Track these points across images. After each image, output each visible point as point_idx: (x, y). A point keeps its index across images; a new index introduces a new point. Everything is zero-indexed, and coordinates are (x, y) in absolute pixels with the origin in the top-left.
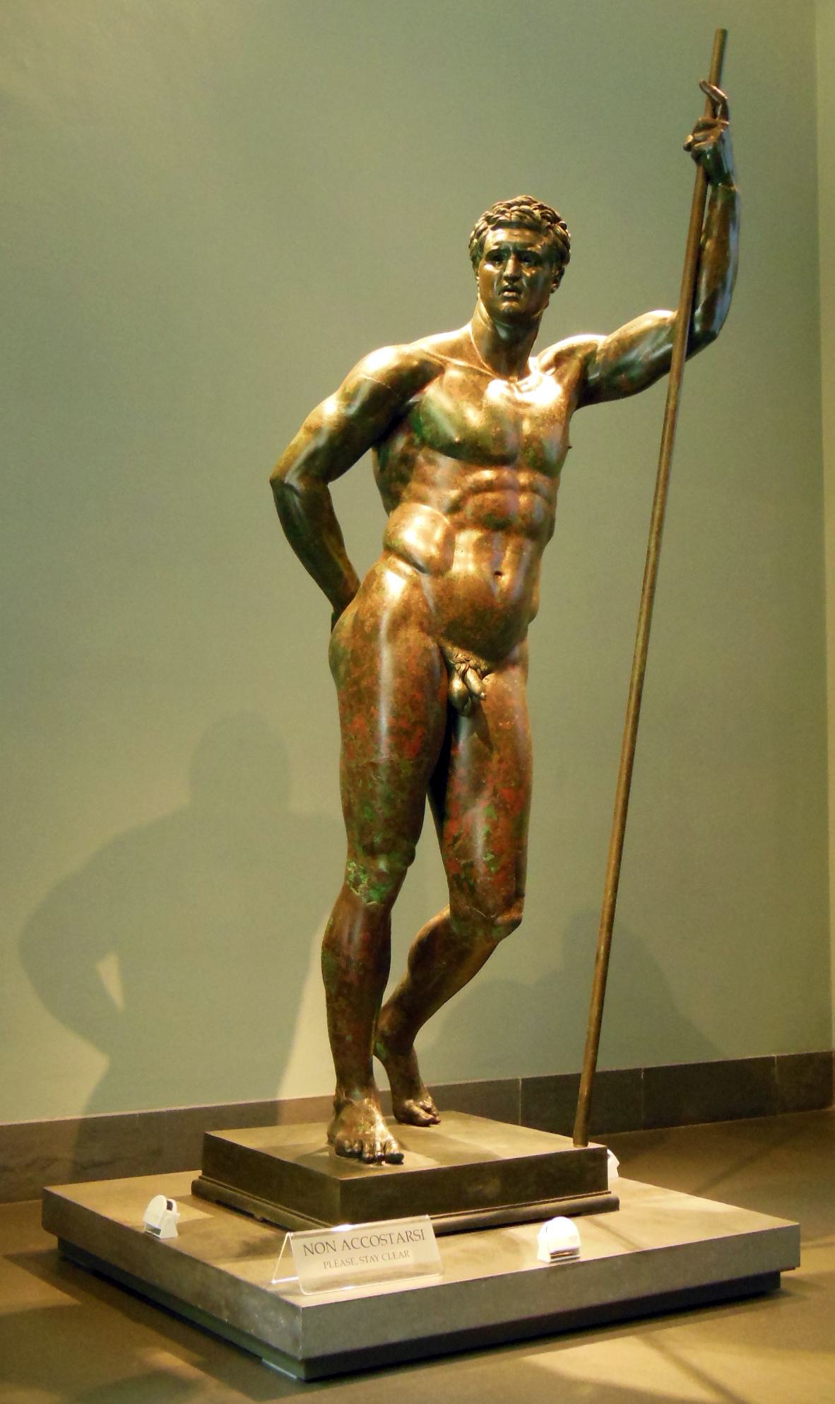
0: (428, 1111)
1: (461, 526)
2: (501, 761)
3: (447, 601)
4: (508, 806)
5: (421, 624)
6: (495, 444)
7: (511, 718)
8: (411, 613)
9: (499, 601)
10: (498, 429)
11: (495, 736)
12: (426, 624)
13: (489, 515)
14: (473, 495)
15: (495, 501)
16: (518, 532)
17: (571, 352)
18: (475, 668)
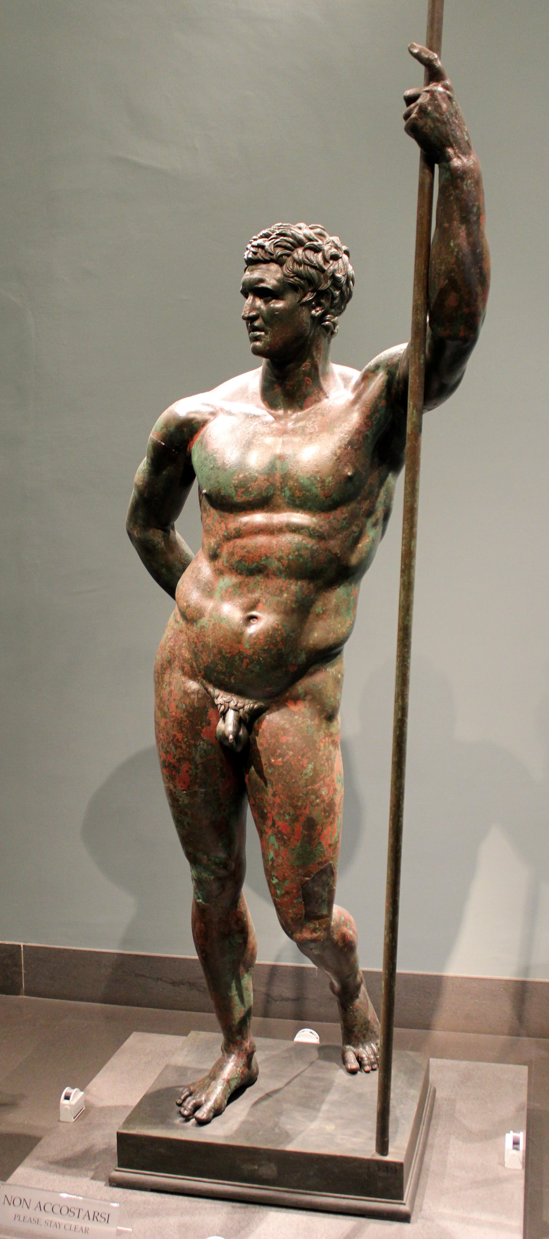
0: (359, 1059)
1: (219, 573)
2: (274, 795)
3: (200, 648)
4: (285, 837)
5: (183, 669)
6: (236, 491)
8: (175, 658)
10: (241, 476)
11: (268, 771)
12: (187, 667)
13: (240, 561)
14: (227, 542)
15: (243, 547)
16: (277, 574)
17: (377, 367)
18: (236, 710)
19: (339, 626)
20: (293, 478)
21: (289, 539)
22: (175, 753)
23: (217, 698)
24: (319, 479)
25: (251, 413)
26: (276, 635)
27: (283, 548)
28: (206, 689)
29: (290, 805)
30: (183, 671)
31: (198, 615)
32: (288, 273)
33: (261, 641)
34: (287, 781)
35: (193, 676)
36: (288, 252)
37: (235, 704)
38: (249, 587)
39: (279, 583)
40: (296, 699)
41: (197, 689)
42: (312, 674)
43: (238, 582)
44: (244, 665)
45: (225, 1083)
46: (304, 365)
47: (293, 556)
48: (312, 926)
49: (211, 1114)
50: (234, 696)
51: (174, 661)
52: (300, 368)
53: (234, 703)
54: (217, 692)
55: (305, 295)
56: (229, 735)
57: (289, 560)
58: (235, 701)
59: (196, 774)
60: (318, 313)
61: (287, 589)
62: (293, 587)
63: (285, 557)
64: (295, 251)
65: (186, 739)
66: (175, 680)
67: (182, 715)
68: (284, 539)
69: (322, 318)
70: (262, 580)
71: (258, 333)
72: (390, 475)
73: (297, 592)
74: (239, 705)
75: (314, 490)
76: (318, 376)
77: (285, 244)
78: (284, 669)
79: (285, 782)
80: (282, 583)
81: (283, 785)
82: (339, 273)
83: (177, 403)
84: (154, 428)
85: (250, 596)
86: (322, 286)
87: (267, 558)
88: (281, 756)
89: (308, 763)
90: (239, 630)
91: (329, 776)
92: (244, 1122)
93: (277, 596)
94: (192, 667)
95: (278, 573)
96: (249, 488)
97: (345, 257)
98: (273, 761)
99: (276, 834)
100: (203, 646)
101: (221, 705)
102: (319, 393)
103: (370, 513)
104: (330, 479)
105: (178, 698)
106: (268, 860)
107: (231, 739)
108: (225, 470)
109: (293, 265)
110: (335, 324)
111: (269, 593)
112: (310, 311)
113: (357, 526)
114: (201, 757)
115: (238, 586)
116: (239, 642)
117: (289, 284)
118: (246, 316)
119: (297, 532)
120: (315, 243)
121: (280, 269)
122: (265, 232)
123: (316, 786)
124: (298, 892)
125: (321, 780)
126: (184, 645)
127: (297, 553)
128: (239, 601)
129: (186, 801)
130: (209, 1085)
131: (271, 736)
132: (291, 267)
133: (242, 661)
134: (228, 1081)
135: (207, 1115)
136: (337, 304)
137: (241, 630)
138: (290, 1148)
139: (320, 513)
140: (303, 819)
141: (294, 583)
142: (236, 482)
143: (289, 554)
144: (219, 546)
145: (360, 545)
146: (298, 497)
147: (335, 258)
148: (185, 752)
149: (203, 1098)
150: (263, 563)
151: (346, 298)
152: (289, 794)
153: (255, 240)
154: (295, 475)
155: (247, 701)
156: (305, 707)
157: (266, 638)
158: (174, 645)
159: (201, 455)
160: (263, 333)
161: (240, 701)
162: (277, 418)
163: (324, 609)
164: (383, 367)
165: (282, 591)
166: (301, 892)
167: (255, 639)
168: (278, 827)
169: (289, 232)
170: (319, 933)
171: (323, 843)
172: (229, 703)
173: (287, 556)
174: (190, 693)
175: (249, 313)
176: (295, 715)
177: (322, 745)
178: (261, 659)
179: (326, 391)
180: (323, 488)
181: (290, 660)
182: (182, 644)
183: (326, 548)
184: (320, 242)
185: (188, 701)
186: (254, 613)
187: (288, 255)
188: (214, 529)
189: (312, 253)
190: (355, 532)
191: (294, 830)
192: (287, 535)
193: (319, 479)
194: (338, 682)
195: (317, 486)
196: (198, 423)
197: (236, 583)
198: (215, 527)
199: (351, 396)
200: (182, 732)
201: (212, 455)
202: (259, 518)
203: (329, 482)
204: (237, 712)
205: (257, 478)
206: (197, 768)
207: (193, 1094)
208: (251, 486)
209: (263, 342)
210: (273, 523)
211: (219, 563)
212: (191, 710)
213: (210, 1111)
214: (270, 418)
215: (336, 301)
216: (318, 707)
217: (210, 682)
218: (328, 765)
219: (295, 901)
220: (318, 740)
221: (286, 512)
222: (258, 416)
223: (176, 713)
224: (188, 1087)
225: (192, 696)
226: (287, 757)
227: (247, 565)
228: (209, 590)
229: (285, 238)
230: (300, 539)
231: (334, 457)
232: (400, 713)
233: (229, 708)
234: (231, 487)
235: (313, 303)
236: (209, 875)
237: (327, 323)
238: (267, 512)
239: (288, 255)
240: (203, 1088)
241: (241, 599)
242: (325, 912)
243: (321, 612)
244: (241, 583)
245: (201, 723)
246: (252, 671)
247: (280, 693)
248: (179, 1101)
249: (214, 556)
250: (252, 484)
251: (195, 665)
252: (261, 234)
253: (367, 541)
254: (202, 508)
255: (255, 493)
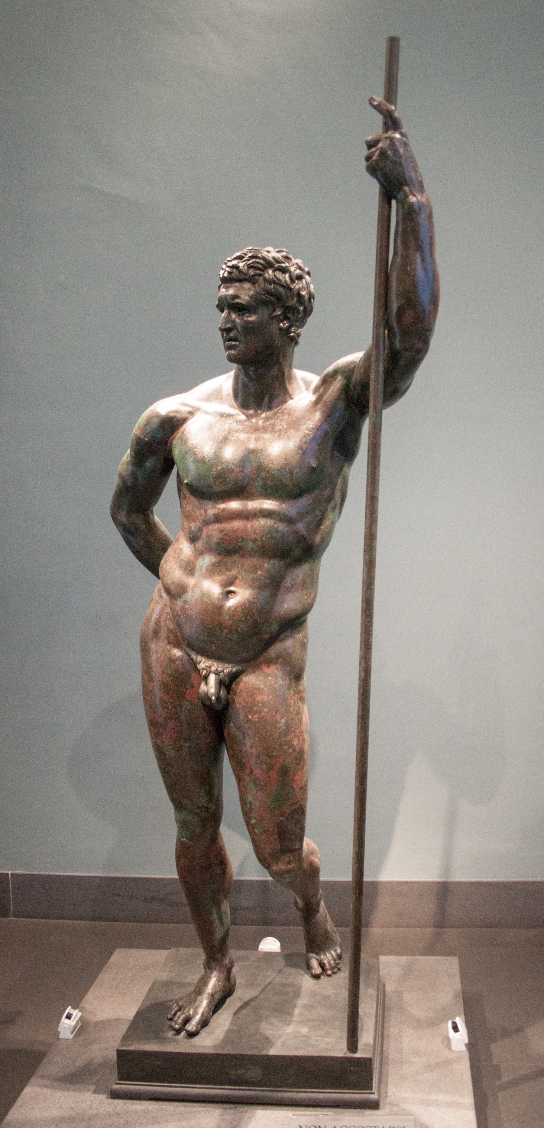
1: (199, 553)
4: (262, 783)
5: (168, 638)
7: (258, 712)
8: (160, 629)
9: (227, 618)
10: (219, 468)
16: (252, 553)
17: (335, 373)
18: (217, 673)
19: (306, 598)
20: (265, 470)
21: (262, 523)
22: (162, 713)
23: (199, 664)
24: (288, 470)
25: (226, 412)
26: (252, 608)
27: (257, 531)
28: (189, 656)
29: (266, 756)
30: (168, 641)
31: (182, 591)
32: (260, 290)
33: (239, 613)
34: (264, 734)
35: (177, 645)
36: (259, 272)
37: (216, 668)
38: (227, 566)
39: (254, 562)
40: (269, 662)
41: (181, 656)
42: (283, 640)
43: (217, 561)
44: (224, 633)
45: (210, 997)
46: (272, 370)
47: (266, 538)
48: (287, 859)
49: (200, 1026)
50: (215, 661)
51: (160, 632)
52: (269, 374)
53: (215, 667)
54: (199, 658)
55: (274, 310)
56: (212, 697)
57: (262, 541)
58: (215, 666)
59: (182, 730)
60: (285, 326)
61: (261, 567)
62: (266, 565)
63: (259, 539)
64: (266, 272)
65: (172, 701)
66: (160, 649)
67: (168, 679)
68: (257, 524)
69: (288, 330)
70: (238, 559)
71: (233, 343)
72: (346, 465)
73: (269, 570)
74: (220, 669)
75: (284, 480)
76: (284, 379)
77: (257, 265)
78: (259, 637)
79: (262, 735)
80: (256, 562)
81: (259, 738)
82: (303, 291)
83: (157, 402)
84: (137, 426)
85: (228, 573)
86: (289, 302)
87: (243, 540)
88: (256, 712)
89: (281, 718)
90: (219, 604)
91: (299, 728)
92: (229, 1031)
93: (252, 573)
94: (176, 636)
95: (253, 553)
96: (226, 478)
97: (307, 277)
98: (250, 717)
99: (254, 781)
100: (186, 618)
101: (203, 669)
102: (285, 395)
103: (330, 499)
104: (298, 470)
105: (164, 664)
106: (247, 803)
107: (214, 700)
108: (205, 463)
109: (265, 285)
110: (298, 335)
111: (245, 570)
112: (279, 323)
113: (320, 510)
114: (185, 716)
115: (217, 565)
116: (220, 614)
117: (261, 300)
118: (223, 327)
119: (269, 517)
120: (283, 265)
121: (252, 287)
122: (238, 254)
123: (289, 738)
124: (274, 830)
125: (292, 733)
126: (168, 617)
127: (269, 535)
128: (218, 578)
129: (173, 755)
130: (196, 1000)
131: (249, 696)
132: (263, 286)
133: (222, 631)
134: (212, 995)
135: (196, 1028)
136: (301, 318)
137: (221, 603)
138: (272, 1052)
139: (288, 500)
140: (278, 766)
141: (267, 562)
142: (215, 473)
143: (262, 536)
144: (200, 530)
145: (322, 527)
146: (270, 487)
147: (300, 278)
148: (171, 712)
149: (191, 1012)
150: (239, 544)
151: (308, 312)
152: (265, 745)
153: (229, 261)
154: (267, 467)
155: (226, 665)
156: (277, 669)
157: (243, 610)
158: (160, 618)
159: (182, 449)
160: (237, 343)
161: (220, 666)
162: (249, 417)
163: (292, 583)
164: (341, 373)
165: (256, 569)
166: (276, 830)
167: (233, 611)
168: (255, 775)
169: (260, 255)
170: (293, 865)
171: (295, 786)
172: (210, 667)
173: (261, 539)
174: (175, 660)
175: (225, 325)
176: (268, 676)
177: (292, 701)
178: (239, 629)
179: (291, 393)
180: (291, 478)
181: (264, 628)
182: (167, 616)
183: (294, 531)
184: (287, 264)
185: (173, 667)
186: (232, 588)
187: (260, 275)
188: (194, 515)
189: (281, 273)
190: (318, 516)
191: (270, 777)
192: (260, 520)
193: (288, 470)
194: (304, 646)
195: (286, 477)
196: (178, 421)
197: (215, 562)
198: (195, 513)
199: (313, 398)
200: (168, 694)
201: (192, 450)
202: (234, 505)
203: (297, 473)
204: (218, 676)
205: (233, 470)
206: (182, 726)
207: (182, 1009)
208: (228, 477)
209: (237, 351)
210: (248, 510)
211: (200, 544)
212: (176, 675)
213: (198, 1024)
214: (243, 417)
215: (300, 316)
216: (288, 668)
217: (193, 649)
218: (298, 719)
219: (271, 838)
220: (289, 698)
221: (259, 499)
222: (232, 415)
223: (162, 678)
224: (177, 1001)
225: (177, 662)
226: (263, 714)
227: (225, 546)
228: (190, 568)
229: (257, 260)
230: (272, 523)
231: (300, 451)
232: (363, 674)
233: (210, 672)
234: (210, 478)
235: (281, 317)
236: (192, 818)
237: (292, 334)
238: (242, 500)
239: (260, 275)
240: (190, 1002)
241: (219, 576)
242: (297, 846)
243: (290, 586)
244: (219, 562)
245: (185, 686)
246: (231, 640)
247: (255, 658)
248: (170, 1016)
249: (193, 539)
250: (229, 475)
251: (179, 634)
252: (235, 256)
253: (328, 523)
254: (182, 496)
255: (232, 483)
